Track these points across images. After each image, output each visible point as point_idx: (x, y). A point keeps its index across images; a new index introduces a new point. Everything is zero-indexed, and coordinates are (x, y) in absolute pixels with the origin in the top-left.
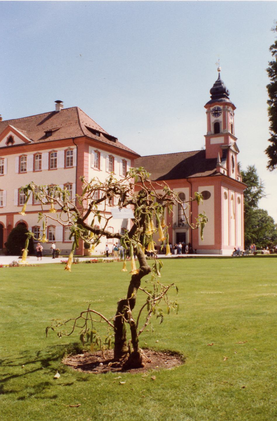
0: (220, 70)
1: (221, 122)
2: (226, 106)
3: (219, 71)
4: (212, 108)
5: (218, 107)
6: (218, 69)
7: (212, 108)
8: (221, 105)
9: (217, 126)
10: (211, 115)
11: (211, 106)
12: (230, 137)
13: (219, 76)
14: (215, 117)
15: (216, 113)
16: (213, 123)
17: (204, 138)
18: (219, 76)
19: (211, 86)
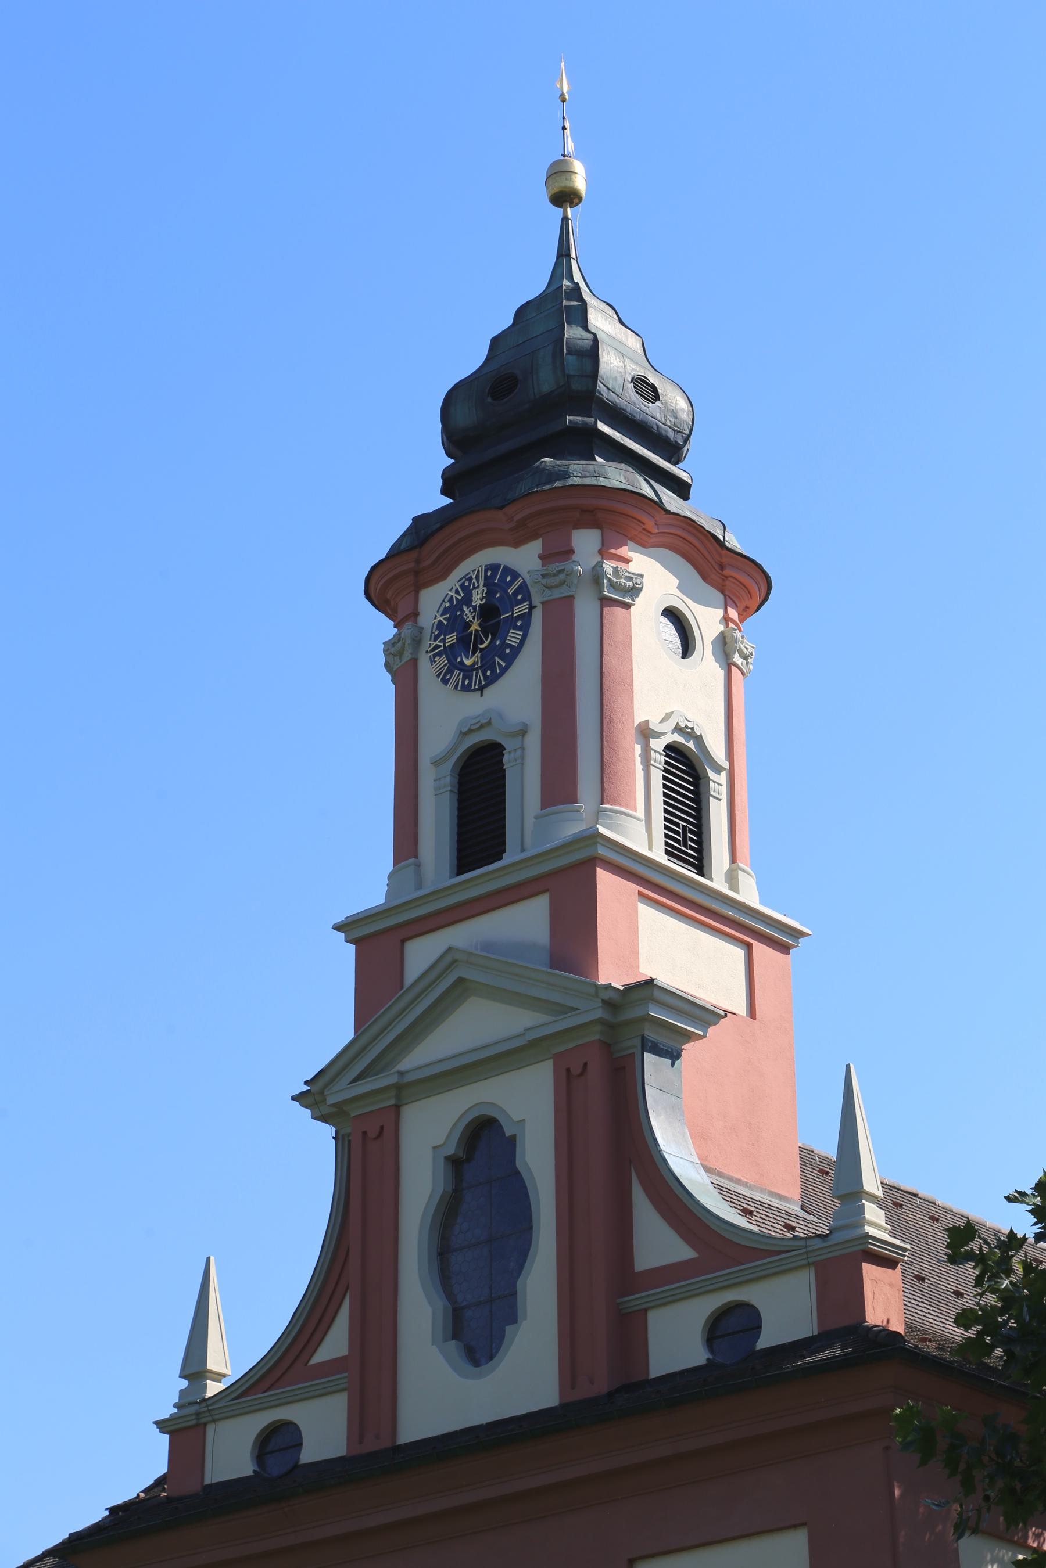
0: (580, 183)
1: (523, 732)
2: (585, 542)
3: (565, 198)
4: (433, 601)
5: (494, 568)
6: (559, 170)
7: (433, 601)
8: (518, 538)
9: (480, 777)
10: (428, 671)
11: (422, 579)
12: (605, 879)
13: (563, 253)
14: (466, 688)
15: (480, 639)
16: (436, 763)
17: (344, 955)
18: (563, 253)
19: (469, 358)
